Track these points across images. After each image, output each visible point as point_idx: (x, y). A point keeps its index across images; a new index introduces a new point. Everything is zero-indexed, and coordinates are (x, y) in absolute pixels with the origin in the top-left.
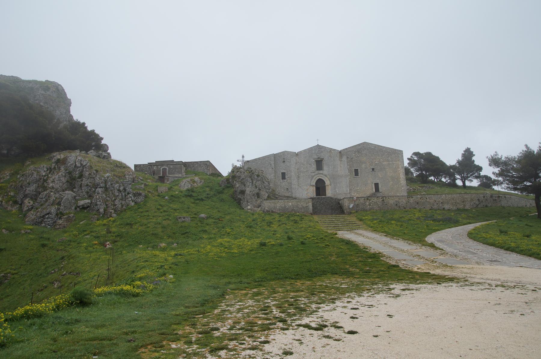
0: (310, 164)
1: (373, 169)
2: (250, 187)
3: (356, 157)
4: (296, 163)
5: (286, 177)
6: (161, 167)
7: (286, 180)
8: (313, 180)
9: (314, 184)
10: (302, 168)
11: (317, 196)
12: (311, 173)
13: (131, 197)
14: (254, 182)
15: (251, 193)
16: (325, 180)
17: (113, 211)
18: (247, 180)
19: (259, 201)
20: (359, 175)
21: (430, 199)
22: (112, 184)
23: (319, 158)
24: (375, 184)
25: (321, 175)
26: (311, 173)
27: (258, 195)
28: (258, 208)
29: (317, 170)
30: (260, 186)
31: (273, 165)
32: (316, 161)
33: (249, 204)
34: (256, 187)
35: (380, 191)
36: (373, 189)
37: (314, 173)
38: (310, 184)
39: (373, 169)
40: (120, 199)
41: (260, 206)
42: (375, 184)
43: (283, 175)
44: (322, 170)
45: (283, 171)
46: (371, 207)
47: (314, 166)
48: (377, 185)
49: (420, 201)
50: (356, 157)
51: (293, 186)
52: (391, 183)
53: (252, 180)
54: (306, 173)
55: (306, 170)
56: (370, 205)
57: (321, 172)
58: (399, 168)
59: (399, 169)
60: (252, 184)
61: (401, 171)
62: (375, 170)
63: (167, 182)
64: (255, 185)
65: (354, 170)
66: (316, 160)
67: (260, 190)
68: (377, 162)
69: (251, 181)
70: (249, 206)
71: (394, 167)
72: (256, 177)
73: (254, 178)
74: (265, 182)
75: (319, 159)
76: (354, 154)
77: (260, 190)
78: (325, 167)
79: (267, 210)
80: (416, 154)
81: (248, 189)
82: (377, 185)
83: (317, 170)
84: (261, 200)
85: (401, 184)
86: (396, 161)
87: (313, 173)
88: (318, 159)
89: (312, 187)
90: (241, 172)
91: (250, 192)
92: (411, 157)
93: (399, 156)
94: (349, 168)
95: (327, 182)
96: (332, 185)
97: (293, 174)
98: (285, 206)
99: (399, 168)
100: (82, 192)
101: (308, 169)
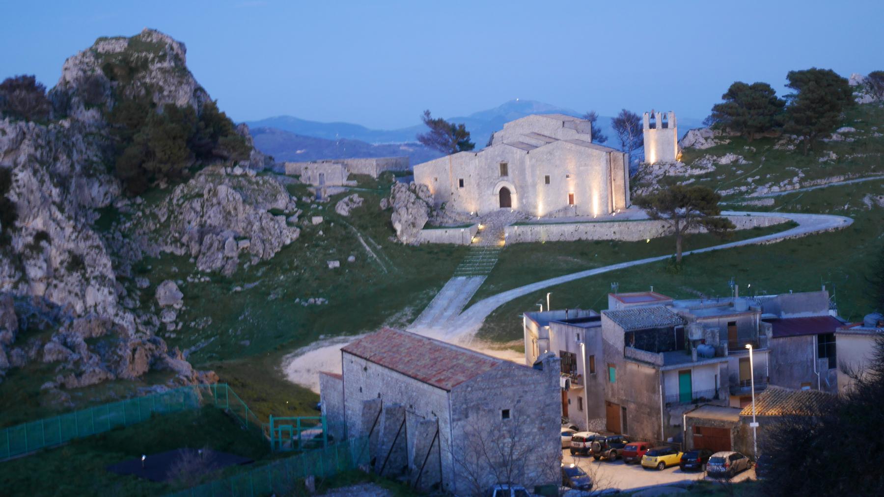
14: (410, 210)
20: (551, 182)
27: (414, 225)
37: (498, 179)
45: (461, 178)
56: (532, 234)
57: (505, 178)
72: (411, 205)
78: (510, 171)
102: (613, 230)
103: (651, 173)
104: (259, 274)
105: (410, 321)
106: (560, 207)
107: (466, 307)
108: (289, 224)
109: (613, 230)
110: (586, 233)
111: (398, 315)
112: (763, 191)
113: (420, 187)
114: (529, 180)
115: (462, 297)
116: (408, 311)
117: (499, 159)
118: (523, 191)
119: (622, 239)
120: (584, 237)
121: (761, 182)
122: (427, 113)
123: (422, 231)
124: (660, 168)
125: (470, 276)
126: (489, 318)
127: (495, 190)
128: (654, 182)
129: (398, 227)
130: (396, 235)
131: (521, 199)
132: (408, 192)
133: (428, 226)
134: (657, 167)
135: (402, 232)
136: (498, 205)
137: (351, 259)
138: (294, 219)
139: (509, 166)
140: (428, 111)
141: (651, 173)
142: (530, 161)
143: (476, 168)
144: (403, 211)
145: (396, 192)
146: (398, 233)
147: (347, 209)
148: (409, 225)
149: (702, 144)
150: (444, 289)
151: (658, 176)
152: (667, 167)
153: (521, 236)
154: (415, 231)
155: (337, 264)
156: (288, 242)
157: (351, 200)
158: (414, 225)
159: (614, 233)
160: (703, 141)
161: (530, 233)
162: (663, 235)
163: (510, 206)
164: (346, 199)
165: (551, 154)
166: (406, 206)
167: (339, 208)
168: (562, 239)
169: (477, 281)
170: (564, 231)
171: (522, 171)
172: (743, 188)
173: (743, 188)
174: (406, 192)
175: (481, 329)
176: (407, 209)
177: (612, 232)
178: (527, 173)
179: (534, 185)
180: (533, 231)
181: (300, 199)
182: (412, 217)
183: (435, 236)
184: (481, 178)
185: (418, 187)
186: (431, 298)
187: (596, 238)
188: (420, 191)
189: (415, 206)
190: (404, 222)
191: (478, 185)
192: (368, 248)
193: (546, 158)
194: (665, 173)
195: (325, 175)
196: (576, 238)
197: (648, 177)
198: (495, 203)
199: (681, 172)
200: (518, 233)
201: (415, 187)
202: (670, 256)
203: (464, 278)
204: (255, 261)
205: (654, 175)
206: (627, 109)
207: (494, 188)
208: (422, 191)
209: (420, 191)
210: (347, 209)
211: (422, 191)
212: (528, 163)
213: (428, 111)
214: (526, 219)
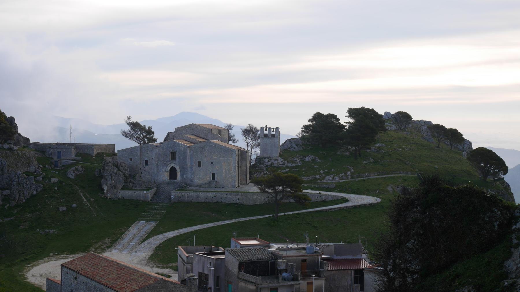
0: (166, 155)
1: (212, 163)
3: (201, 152)
5: (148, 164)
6: (56, 150)
7: (148, 166)
9: (169, 170)
11: (170, 179)
13: (34, 187)
14: (113, 178)
17: (23, 198)
20: (201, 166)
22: (22, 180)
23: (173, 151)
26: (167, 162)
27: (115, 187)
29: (172, 160)
31: (139, 154)
32: (172, 153)
35: (216, 180)
37: (169, 162)
38: (166, 170)
39: (212, 163)
40: (27, 190)
43: (147, 162)
45: (147, 159)
48: (214, 175)
50: (201, 152)
53: (112, 177)
54: (163, 162)
55: (163, 160)
58: (231, 163)
59: (232, 164)
61: (233, 165)
63: (60, 165)
65: (198, 162)
66: (171, 152)
68: (215, 157)
69: (111, 178)
71: (228, 162)
72: (114, 174)
74: (120, 178)
75: (173, 152)
76: (199, 150)
78: (177, 157)
82: (214, 175)
83: (172, 160)
84: (117, 190)
85: (231, 175)
88: (172, 152)
89: (166, 173)
90: (109, 166)
91: (110, 185)
100: (3, 182)
102: (237, 197)
103: (263, 164)
104: (15, 212)
105: (108, 247)
106: (207, 181)
107: (144, 240)
108: (36, 181)
109: (237, 197)
110: (221, 198)
111: (101, 243)
112: (329, 178)
113: (121, 164)
114: (189, 164)
115: (142, 233)
116: (107, 240)
118: (183, 169)
119: (243, 203)
120: (220, 200)
121: (328, 174)
122: (129, 118)
123: (120, 191)
124: (269, 161)
125: (147, 221)
126: (159, 248)
127: (167, 169)
128: (265, 169)
129: (106, 188)
130: (104, 193)
131: (182, 175)
132: (113, 167)
133: (124, 188)
134: (266, 160)
135: (107, 191)
136: (168, 178)
137: (74, 205)
138: (40, 178)
139: (177, 154)
140: (130, 117)
141: (263, 164)
142: (190, 152)
143: (156, 154)
144: (109, 178)
146: (105, 191)
147: (74, 174)
149: (295, 148)
150: (131, 228)
151: (267, 166)
152: (273, 161)
153: (181, 198)
155: (65, 208)
156: (35, 193)
157: (77, 169)
158: (115, 187)
159: (238, 199)
160: (296, 147)
161: (187, 196)
162: (267, 202)
163: (176, 179)
164: (74, 168)
165: (203, 149)
166: (111, 175)
167: (69, 174)
168: (207, 200)
169: (153, 224)
170: (208, 196)
171: (185, 158)
172: (317, 177)
173: (317, 177)
174: (111, 166)
175: (152, 255)
176: (112, 177)
177: (237, 199)
178: (187, 159)
179: (191, 167)
180: (189, 195)
181: (44, 167)
182: (114, 182)
183: (128, 194)
184: (159, 160)
185: (119, 164)
186: (122, 234)
187: (227, 202)
188: (120, 166)
189: (117, 175)
191: (157, 165)
192: (85, 200)
193: (200, 151)
194: (271, 164)
195: (61, 152)
196: (215, 201)
197: (261, 166)
198: (165, 176)
199: (281, 165)
200: (179, 196)
201: (118, 164)
202: (271, 215)
203: (144, 222)
204: (14, 203)
205: (265, 165)
206: (251, 124)
208: (122, 166)
209: (120, 166)
210: (74, 174)
211: (122, 166)
212: (189, 153)
213: (130, 117)
214: (185, 186)
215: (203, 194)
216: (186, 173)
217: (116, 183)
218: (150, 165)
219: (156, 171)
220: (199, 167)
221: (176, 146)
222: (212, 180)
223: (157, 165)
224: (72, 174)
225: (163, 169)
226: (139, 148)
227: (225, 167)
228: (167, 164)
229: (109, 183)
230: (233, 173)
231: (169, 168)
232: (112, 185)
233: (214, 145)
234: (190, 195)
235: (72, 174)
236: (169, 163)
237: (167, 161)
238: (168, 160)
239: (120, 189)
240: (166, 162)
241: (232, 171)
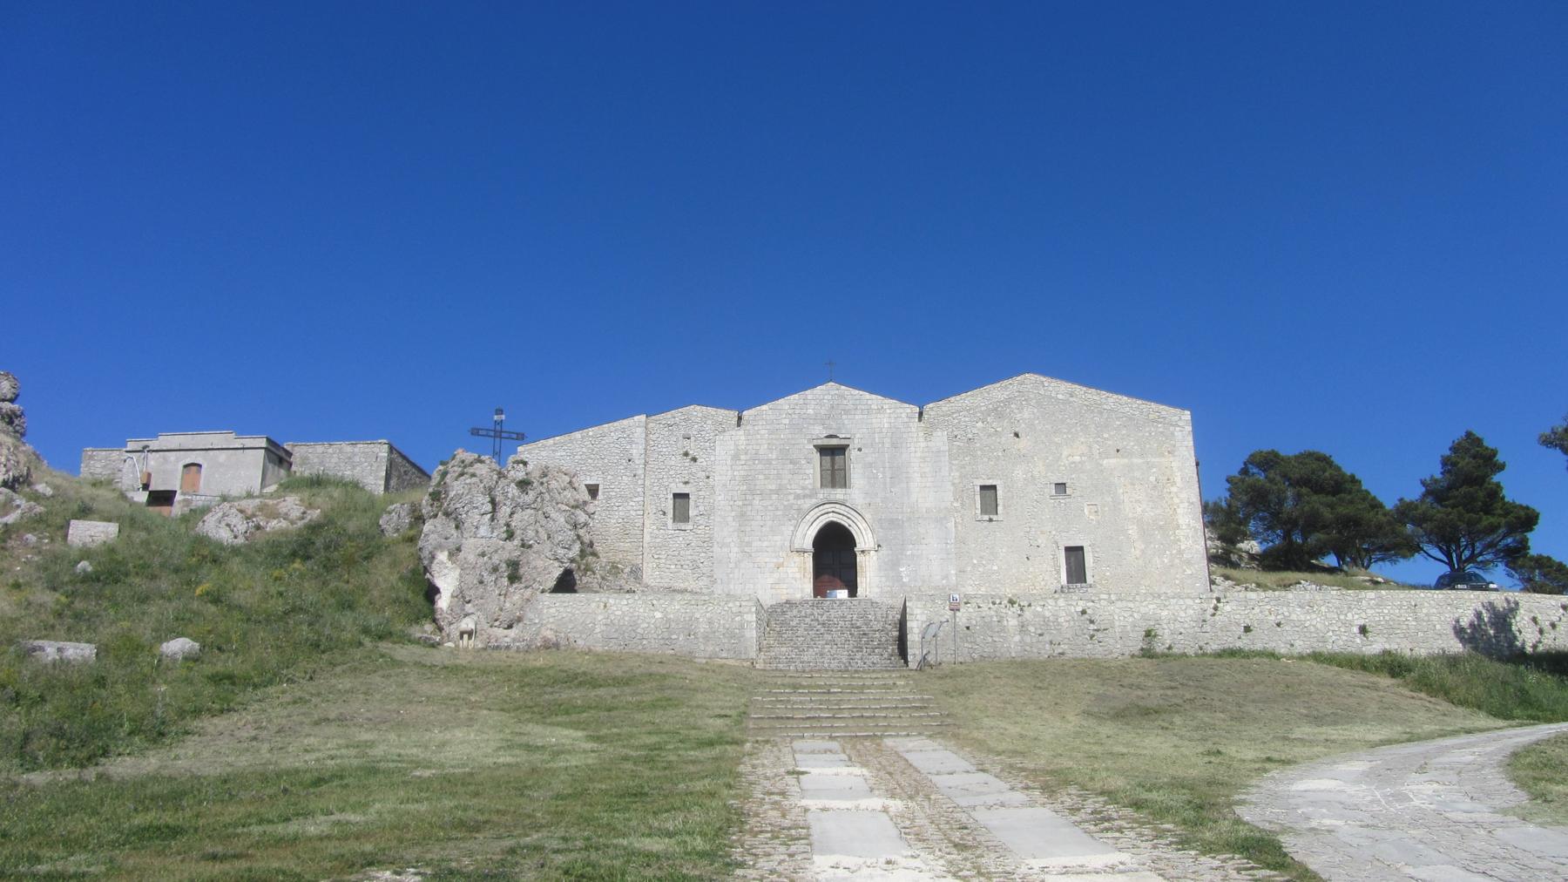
1: (1061, 487)
2: (483, 531)
4: (736, 457)
5: (692, 513)
6: (178, 460)
7: (689, 526)
8: (803, 526)
9: (808, 543)
10: (761, 477)
12: (797, 497)
14: (504, 511)
15: (481, 560)
16: (854, 530)
18: (471, 502)
19: (516, 597)
20: (1000, 508)
21: (1308, 612)
24: (1068, 550)
25: (838, 508)
26: (797, 497)
28: (510, 627)
30: (531, 533)
31: (639, 461)
33: (469, 608)
34: (510, 535)
35: (1089, 579)
36: (1058, 572)
37: (810, 496)
39: (1061, 487)
41: (519, 620)
42: (1068, 550)
44: (844, 485)
46: (1028, 639)
47: (813, 466)
48: (1075, 555)
49: (1261, 621)
51: (716, 548)
52: (1140, 545)
53: (493, 502)
54: (774, 497)
55: (774, 487)
56: (1023, 628)
57: (838, 494)
58: (1174, 484)
59: (1174, 489)
60: (493, 519)
61: (1183, 495)
62: (1069, 491)
64: (508, 525)
66: (819, 442)
67: (530, 546)
68: (1077, 459)
69: (489, 507)
70: (467, 619)
71: (1152, 479)
72: (513, 490)
73: (505, 494)
74: (553, 515)
75: (834, 442)
77: (525, 545)
79: (546, 640)
80: (1268, 461)
81: (472, 540)
82: (1075, 555)
84: (528, 592)
85: (1180, 552)
86: (1162, 455)
87: (805, 496)
89: (797, 558)
91: (483, 555)
92: (1244, 471)
93: (1173, 434)
94: (956, 481)
95: (864, 539)
96: (884, 551)
97: (720, 499)
98: (634, 625)
99: (1174, 484)
101: (785, 482)
117: (819, 433)
127: (799, 534)
131: (892, 565)
135: (461, 597)
136: (808, 587)
145: (448, 479)
146: (443, 602)
148: (495, 569)
154: (517, 594)
159: (1363, 630)
161: (1013, 622)
177: (1356, 630)
190: (472, 558)
191: (742, 516)
207: (797, 527)
215: (1119, 604)
216: (912, 555)
217: (525, 545)
218: (701, 520)
219: (736, 550)
220: (986, 517)
221: (847, 412)
222: (1068, 582)
223: (743, 515)
224: (228, 525)
225: (778, 538)
226: (639, 430)
227: (1139, 510)
228: (799, 510)
229: (471, 547)
230: (1187, 537)
231: (813, 532)
232: (496, 559)
233: (1060, 396)
234: (1037, 615)
235: (228, 525)
236: (814, 501)
237: (799, 492)
238: (803, 488)
239: (552, 583)
240: (791, 497)
241: (1178, 527)
